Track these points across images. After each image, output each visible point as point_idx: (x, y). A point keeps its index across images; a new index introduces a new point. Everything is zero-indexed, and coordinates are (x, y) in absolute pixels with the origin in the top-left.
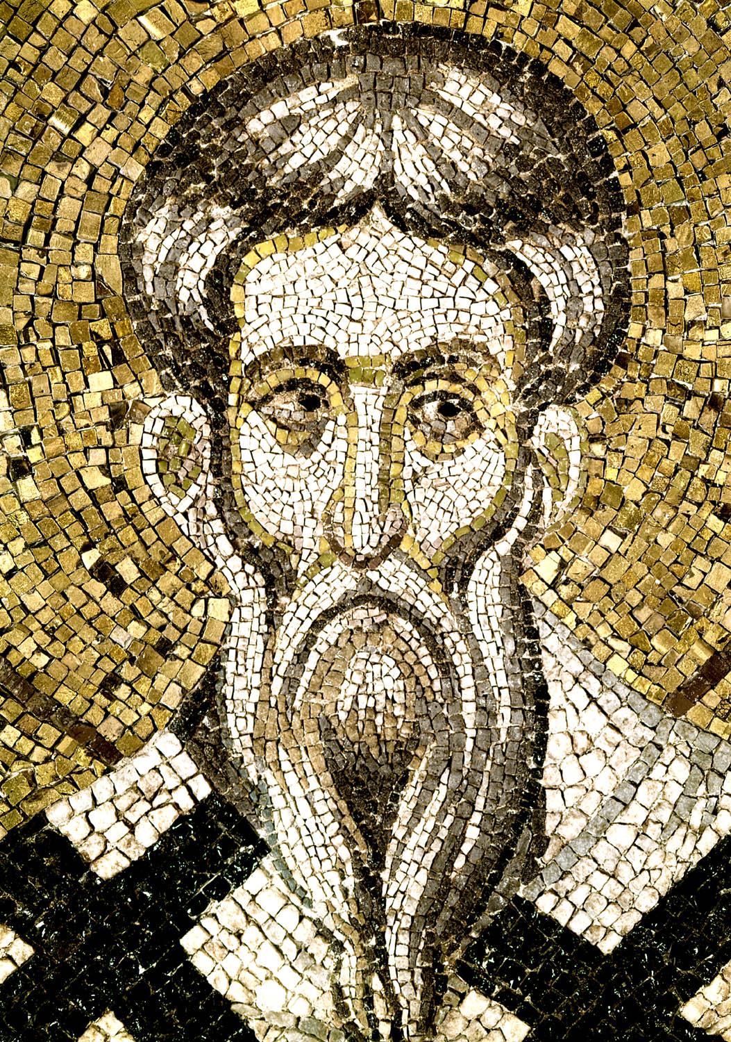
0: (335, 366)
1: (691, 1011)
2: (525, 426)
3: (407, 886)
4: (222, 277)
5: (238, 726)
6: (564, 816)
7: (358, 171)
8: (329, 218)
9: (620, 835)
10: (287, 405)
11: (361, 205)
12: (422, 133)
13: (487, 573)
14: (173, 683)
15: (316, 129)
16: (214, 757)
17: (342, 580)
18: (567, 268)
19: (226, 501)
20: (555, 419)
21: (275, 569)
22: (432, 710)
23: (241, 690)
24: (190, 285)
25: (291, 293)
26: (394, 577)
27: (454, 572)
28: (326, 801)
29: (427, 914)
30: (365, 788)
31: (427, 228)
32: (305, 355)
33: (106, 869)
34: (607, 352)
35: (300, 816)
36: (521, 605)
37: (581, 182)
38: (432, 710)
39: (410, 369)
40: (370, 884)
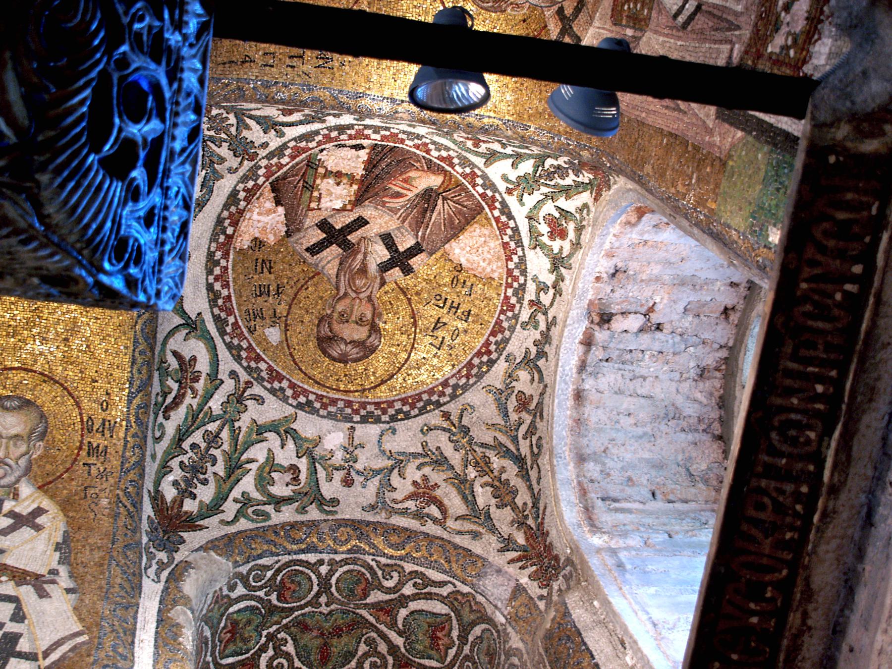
0: (357, 323)
1: (325, 235)
2: (333, 312)
3: (360, 257)
4: (369, 336)
5: (378, 280)
6: (337, 261)
7: (350, 346)
8: (354, 341)
9: (330, 258)
10: (364, 319)
11: (350, 343)
12: (341, 350)
13: (342, 293)
14: (386, 288)
15: (354, 352)
16: (382, 278)
17: (362, 296)
18: (325, 331)
19: (375, 309)
20: (329, 312)
21: (370, 299)
22: (352, 279)
23: (377, 286)
24: (373, 336)
25: (361, 333)
26: (354, 295)
27: (346, 294)
28: (369, 270)
29: (358, 252)
30: (363, 270)
31: (342, 338)
32: (361, 325)
33: (398, 268)
34: (321, 320)
35: (373, 268)
36: (338, 288)
37: (322, 341)
38: (352, 279)
39: (347, 321)
40: (365, 257)
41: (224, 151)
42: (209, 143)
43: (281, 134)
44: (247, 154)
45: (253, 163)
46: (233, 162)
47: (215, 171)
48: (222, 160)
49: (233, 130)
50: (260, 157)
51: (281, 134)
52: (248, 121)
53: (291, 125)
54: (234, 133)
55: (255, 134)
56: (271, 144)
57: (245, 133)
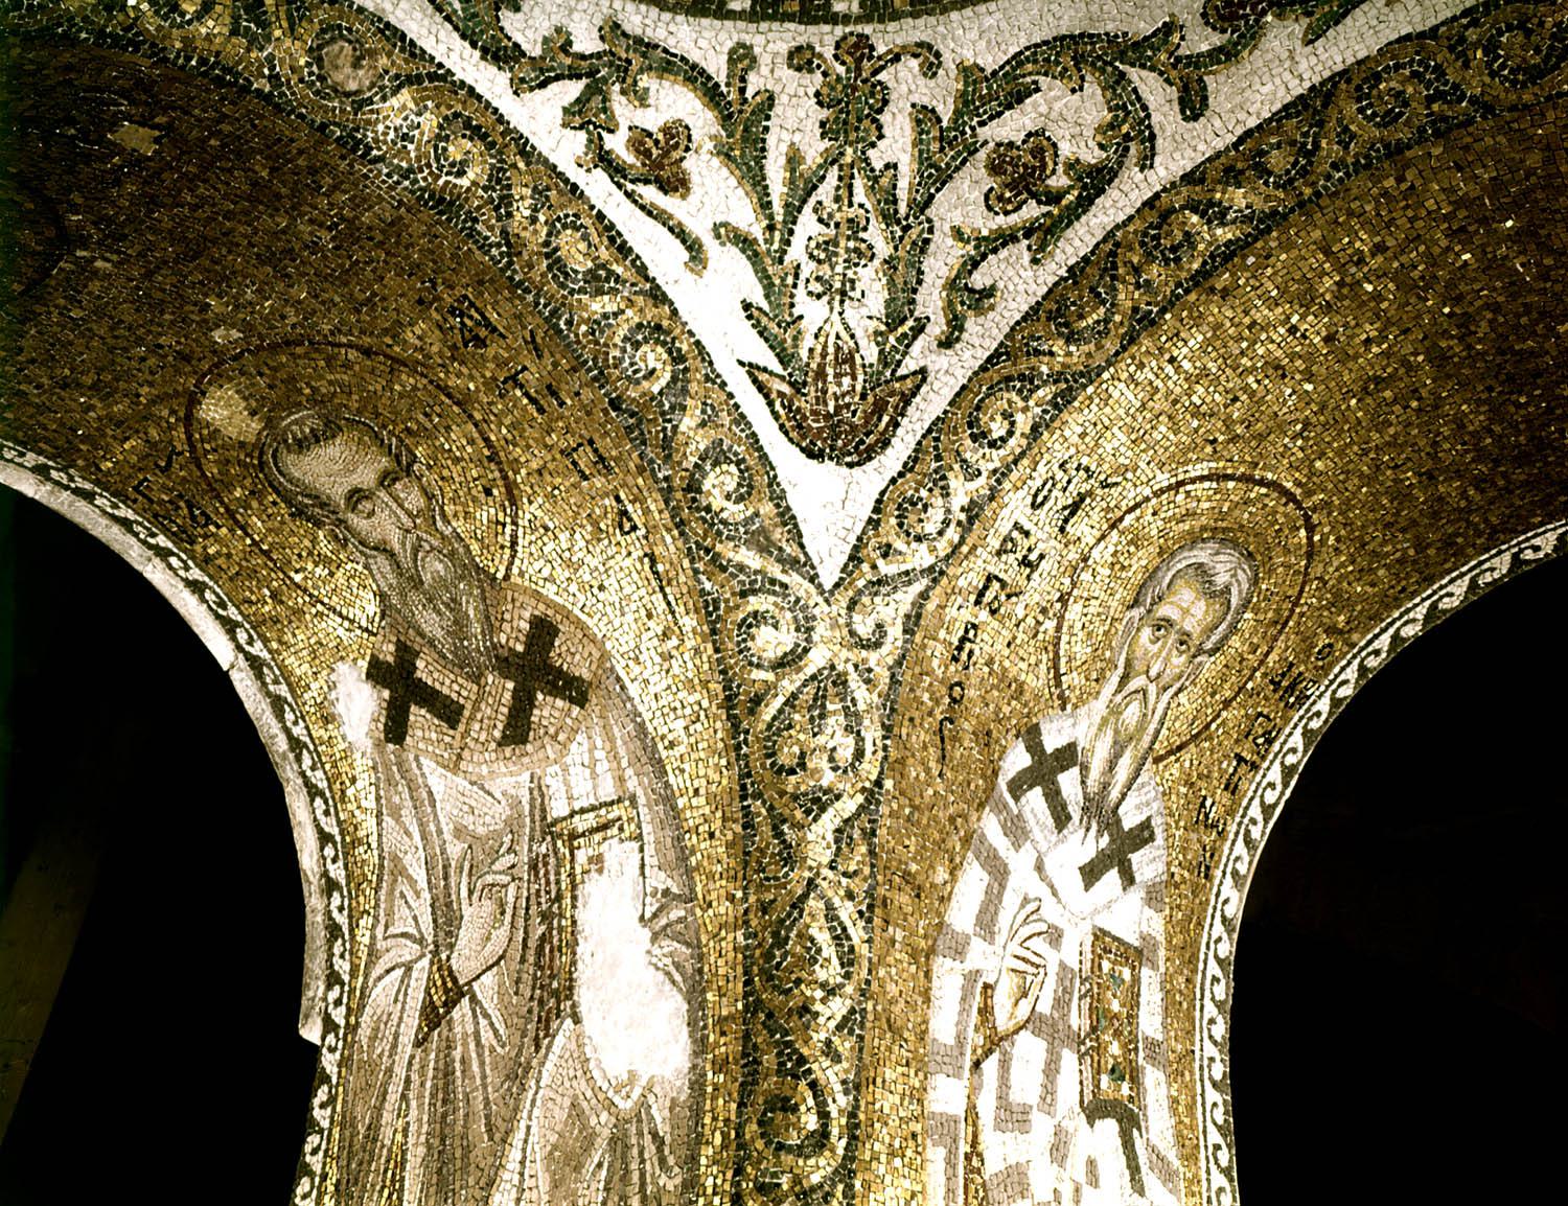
41: (896, 145)
42: (903, 208)
43: (742, 59)
44: (859, 70)
45: (868, 29)
46: (906, 83)
47: (966, 104)
48: (924, 116)
49: (825, 192)
50: (839, 31)
51: (742, 59)
52: (777, 189)
53: (695, 76)
54: (833, 175)
55: (797, 125)
56: (783, 48)
57: (814, 149)
